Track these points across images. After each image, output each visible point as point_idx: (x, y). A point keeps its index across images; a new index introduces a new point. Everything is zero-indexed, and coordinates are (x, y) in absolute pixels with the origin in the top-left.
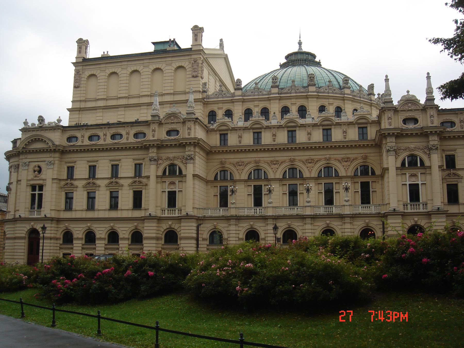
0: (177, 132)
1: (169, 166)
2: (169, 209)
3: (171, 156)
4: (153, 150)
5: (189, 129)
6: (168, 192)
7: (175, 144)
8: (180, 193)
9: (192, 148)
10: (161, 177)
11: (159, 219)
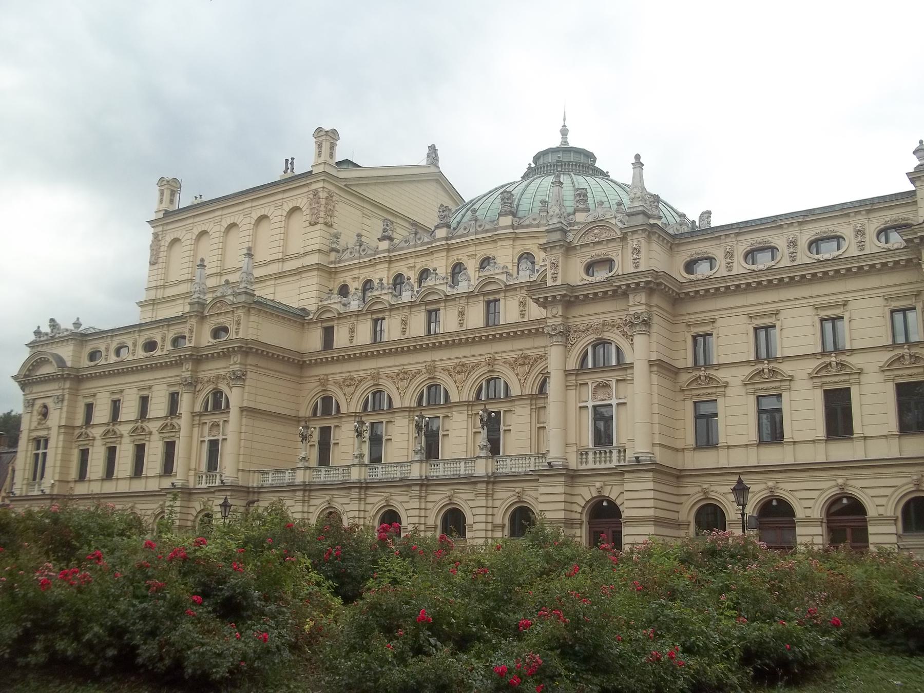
0: (609, 262)
1: (594, 347)
2: (598, 450)
3: (595, 321)
5: (637, 251)
6: (595, 407)
7: (605, 293)
8: (622, 408)
9: (642, 298)
10: (577, 373)
11: (572, 476)
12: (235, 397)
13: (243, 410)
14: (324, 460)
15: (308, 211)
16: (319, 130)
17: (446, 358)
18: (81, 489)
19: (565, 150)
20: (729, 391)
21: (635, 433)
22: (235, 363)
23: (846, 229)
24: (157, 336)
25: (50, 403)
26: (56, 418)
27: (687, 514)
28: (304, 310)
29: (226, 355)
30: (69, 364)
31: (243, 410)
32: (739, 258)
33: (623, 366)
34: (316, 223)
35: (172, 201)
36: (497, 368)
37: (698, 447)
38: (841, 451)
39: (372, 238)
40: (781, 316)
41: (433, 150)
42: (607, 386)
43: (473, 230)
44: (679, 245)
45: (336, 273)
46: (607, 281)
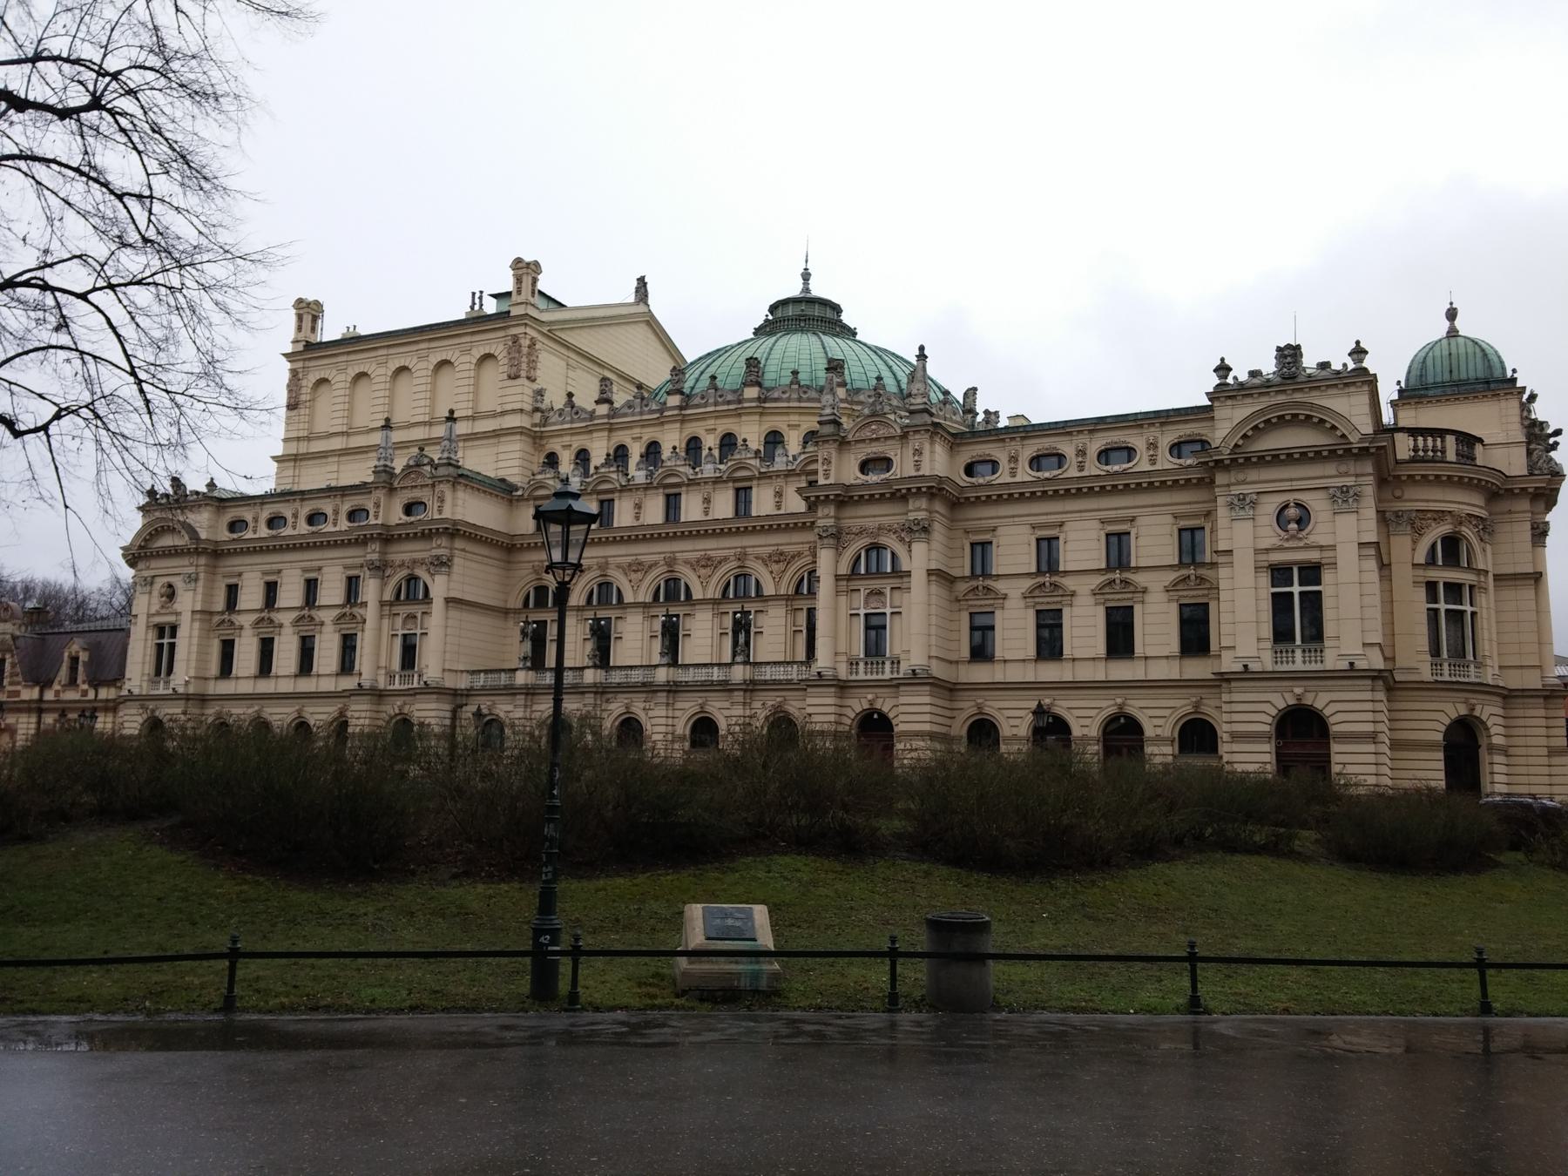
1: (867, 551)
3: (871, 523)
4: (826, 511)
5: (918, 452)
8: (896, 617)
11: (843, 687)
12: (439, 587)
13: (450, 601)
15: (506, 361)
16: (518, 261)
17: (688, 550)
18: (225, 687)
19: (806, 300)
20: (1007, 604)
22: (439, 546)
23: (1138, 441)
24: (327, 507)
25: (178, 583)
26: (187, 601)
27: (960, 729)
28: (503, 480)
29: (427, 536)
30: (203, 536)
31: (448, 601)
32: (1023, 463)
33: (899, 574)
34: (517, 377)
35: (313, 329)
36: (748, 563)
38: (1122, 671)
39: (586, 397)
40: (1065, 528)
41: (642, 282)
42: (880, 593)
43: (711, 401)
44: (959, 445)
45: (541, 438)
46: (887, 482)
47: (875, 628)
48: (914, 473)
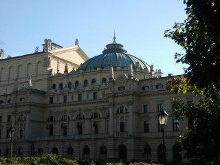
5: (130, 85)
11: (115, 139)
14: (51, 134)
21: (130, 129)
32: (154, 87)
37: (145, 132)
39: (62, 71)
47: (122, 126)
48: (129, 90)
